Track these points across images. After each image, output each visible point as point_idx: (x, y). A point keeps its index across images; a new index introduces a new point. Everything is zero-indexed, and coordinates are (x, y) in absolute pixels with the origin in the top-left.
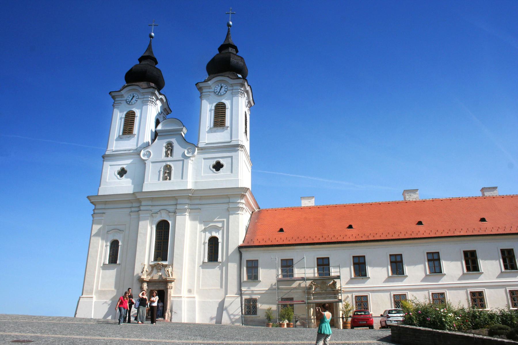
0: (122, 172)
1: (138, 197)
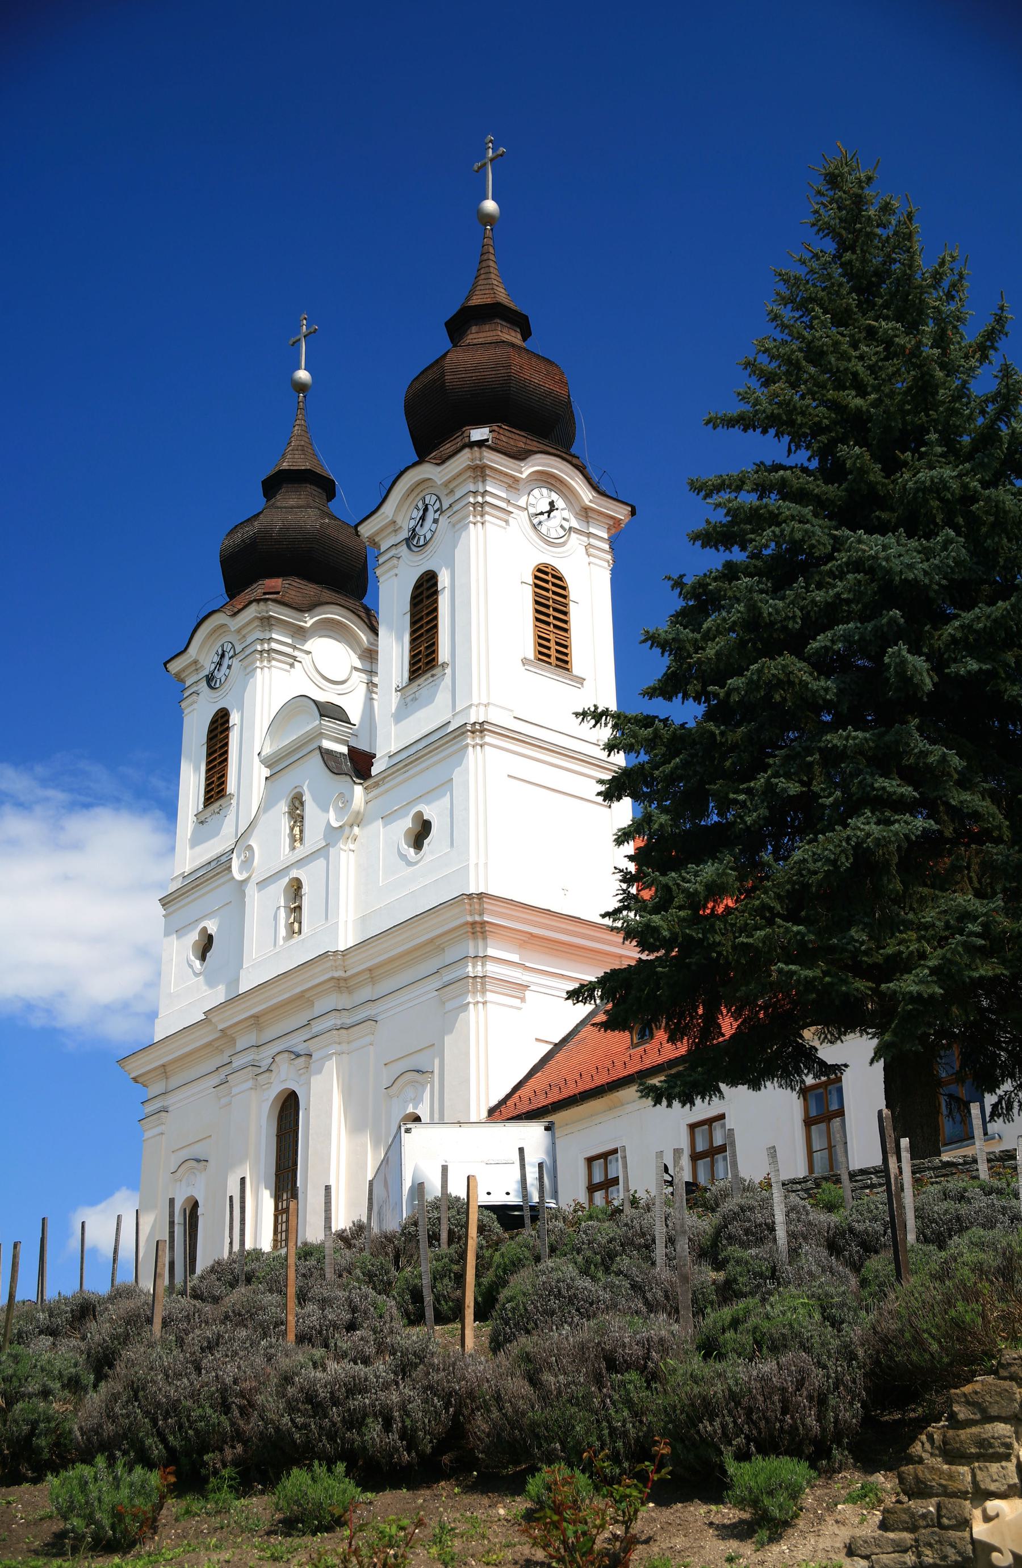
1: (221, 1027)
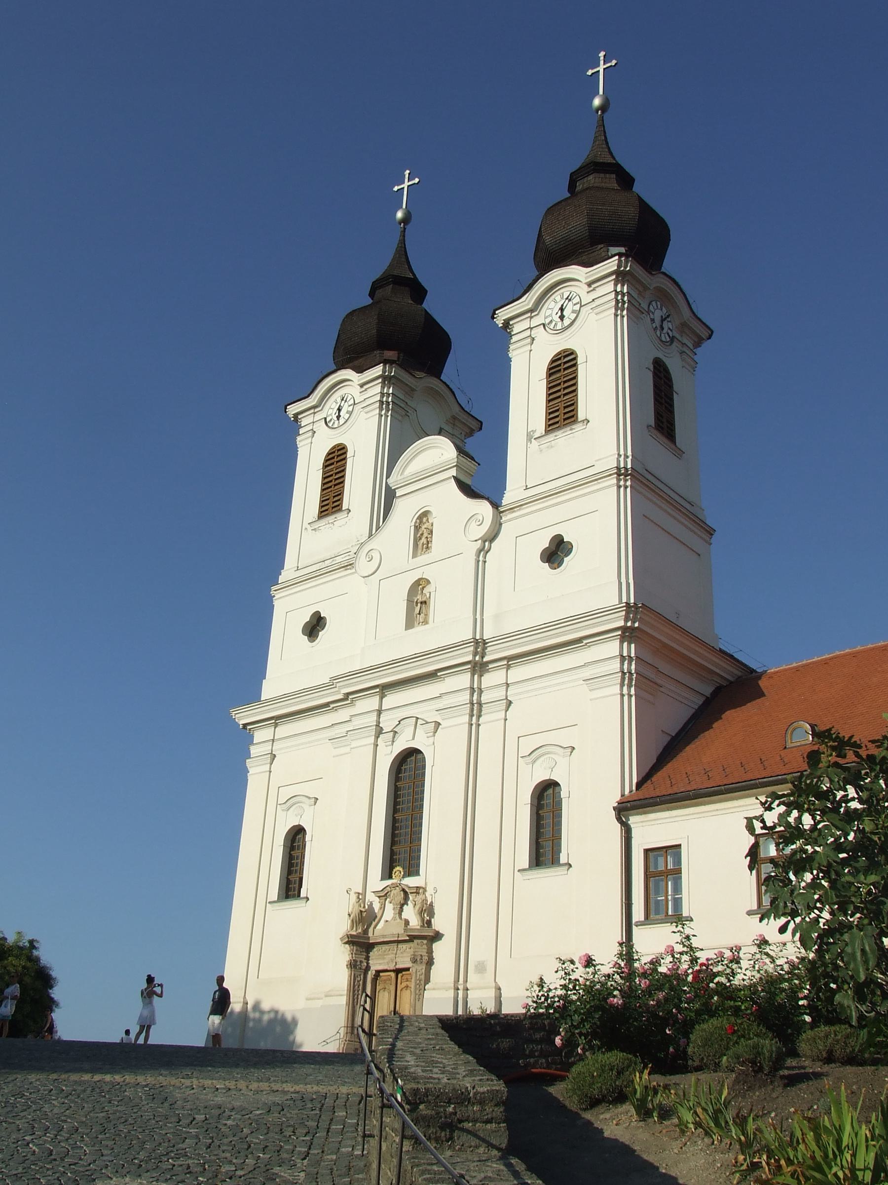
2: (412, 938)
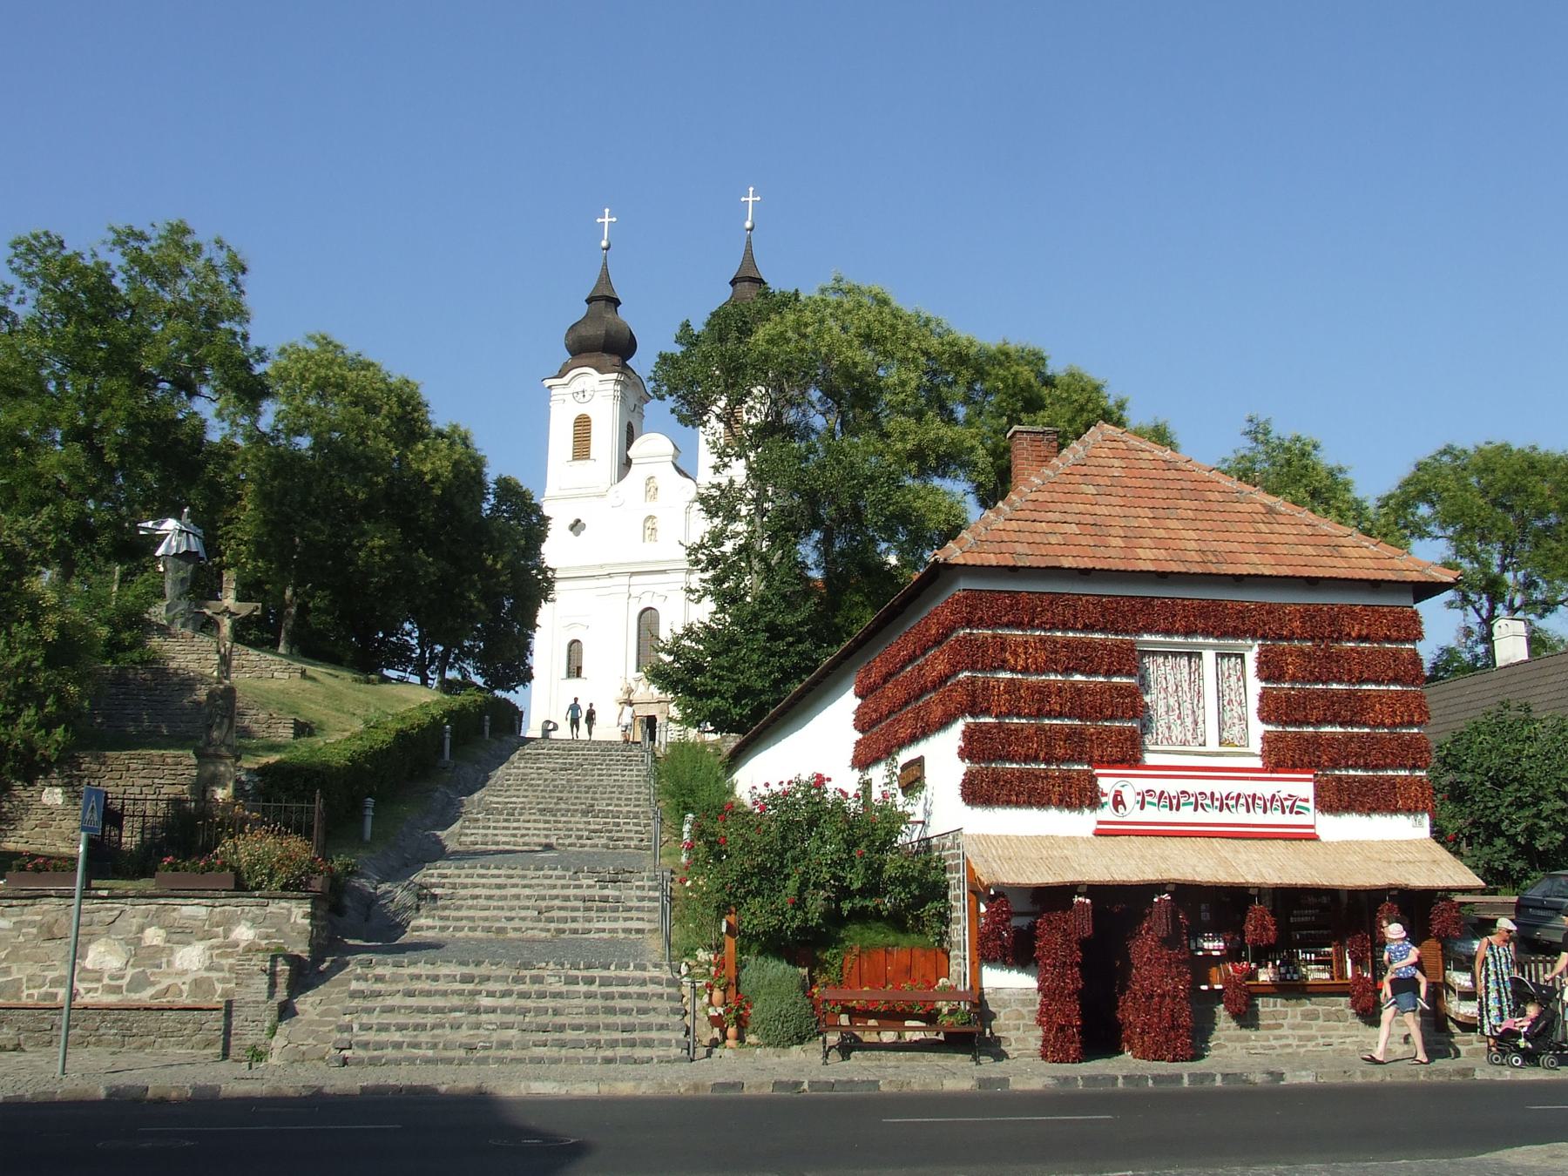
0: (576, 526)
2: (659, 702)
